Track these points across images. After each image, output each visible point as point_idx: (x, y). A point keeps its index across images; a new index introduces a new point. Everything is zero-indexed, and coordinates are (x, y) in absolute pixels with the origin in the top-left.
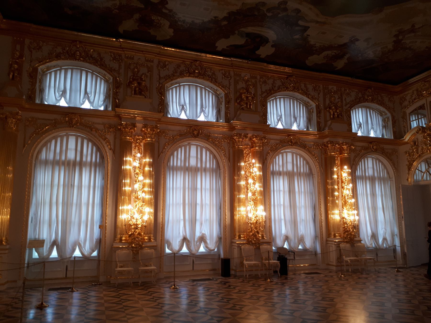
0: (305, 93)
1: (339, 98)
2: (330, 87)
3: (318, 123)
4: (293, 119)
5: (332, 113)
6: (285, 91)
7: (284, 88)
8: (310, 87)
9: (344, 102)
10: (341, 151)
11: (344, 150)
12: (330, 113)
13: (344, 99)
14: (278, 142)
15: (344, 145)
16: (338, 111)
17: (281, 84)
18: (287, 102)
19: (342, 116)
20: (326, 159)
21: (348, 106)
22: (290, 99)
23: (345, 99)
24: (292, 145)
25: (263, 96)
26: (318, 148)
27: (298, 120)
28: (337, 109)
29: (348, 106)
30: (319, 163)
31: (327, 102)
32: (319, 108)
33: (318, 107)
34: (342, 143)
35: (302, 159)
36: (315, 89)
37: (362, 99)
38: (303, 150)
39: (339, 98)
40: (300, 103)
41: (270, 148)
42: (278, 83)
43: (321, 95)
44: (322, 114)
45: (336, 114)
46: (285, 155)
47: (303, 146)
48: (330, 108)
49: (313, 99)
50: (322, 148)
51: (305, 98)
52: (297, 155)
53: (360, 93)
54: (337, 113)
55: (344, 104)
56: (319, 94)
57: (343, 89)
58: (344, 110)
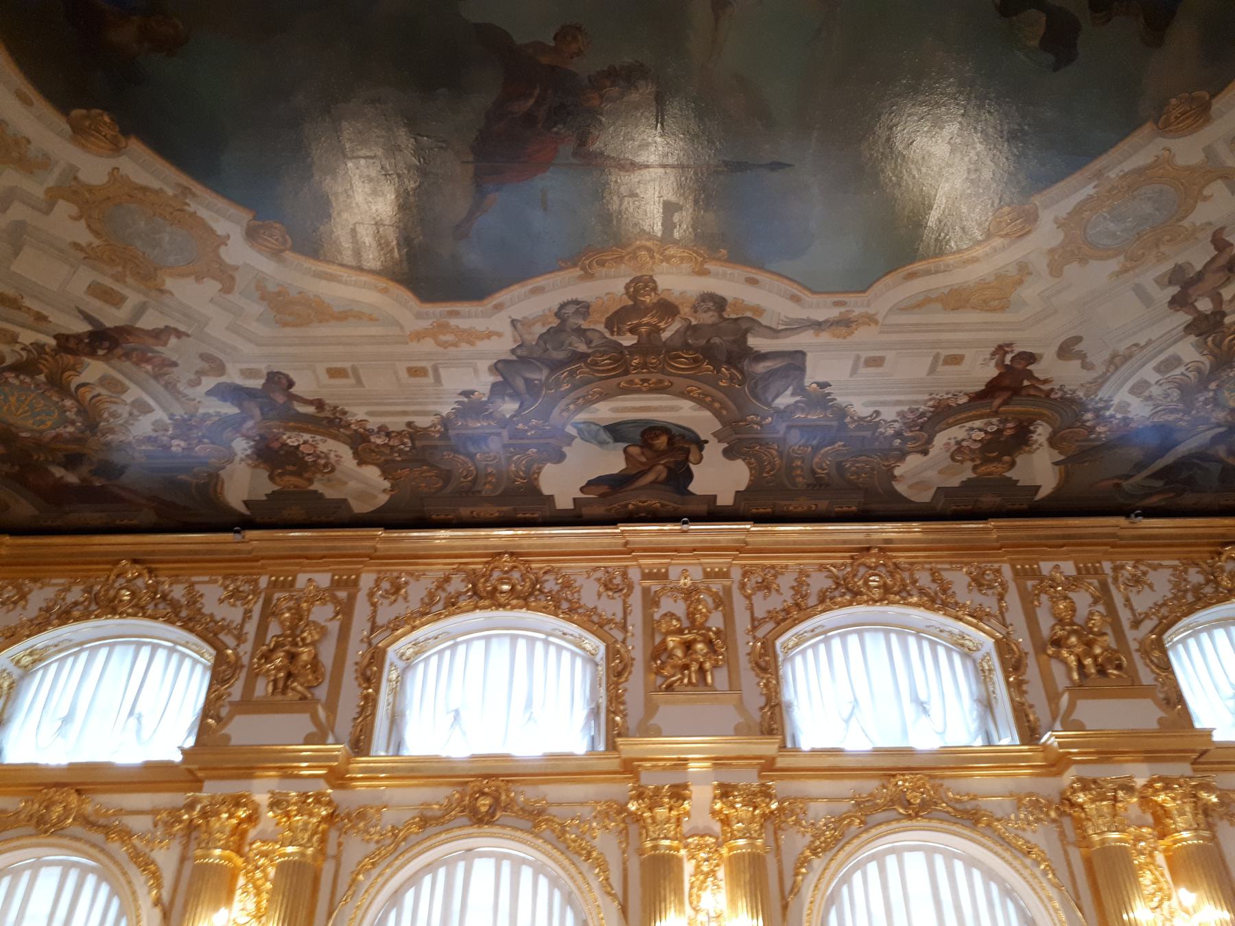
0: (939, 599)
1: (1096, 602)
2: (1046, 567)
3: (1021, 714)
4: (910, 709)
5: (1074, 664)
6: (850, 604)
7: (843, 595)
8: (959, 579)
9: (1125, 616)
10: (1161, 822)
11: (1167, 813)
12: (1064, 662)
13: (1118, 600)
14: (845, 807)
15: (1156, 792)
16: (1098, 651)
17: (830, 583)
18: (875, 642)
19: (1119, 667)
20: (1089, 863)
21: (1148, 625)
22: (887, 633)
23: (1128, 600)
24: (909, 817)
25: (760, 633)
26: (1038, 820)
27: (935, 707)
28: (1089, 644)
29: (1148, 625)
30: (1058, 887)
31: (1046, 623)
32: (1011, 651)
33: (1003, 646)
34: (1150, 785)
35: (976, 874)
36: (978, 582)
37: (1208, 590)
38: (967, 832)
39: (1096, 602)
40: (933, 644)
41: (808, 838)
42: (819, 582)
43: (1013, 599)
44: (1032, 671)
45: (1088, 661)
46: (891, 861)
47: (969, 817)
48: (1058, 643)
49: (979, 616)
50: (1062, 814)
51: (938, 619)
52: (949, 857)
53: (1192, 571)
54: (1095, 658)
55: (1126, 624)
56: (1001, 598)
57: (1107, 566)
58: (1134, 646)
